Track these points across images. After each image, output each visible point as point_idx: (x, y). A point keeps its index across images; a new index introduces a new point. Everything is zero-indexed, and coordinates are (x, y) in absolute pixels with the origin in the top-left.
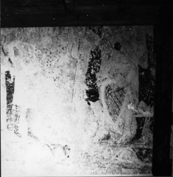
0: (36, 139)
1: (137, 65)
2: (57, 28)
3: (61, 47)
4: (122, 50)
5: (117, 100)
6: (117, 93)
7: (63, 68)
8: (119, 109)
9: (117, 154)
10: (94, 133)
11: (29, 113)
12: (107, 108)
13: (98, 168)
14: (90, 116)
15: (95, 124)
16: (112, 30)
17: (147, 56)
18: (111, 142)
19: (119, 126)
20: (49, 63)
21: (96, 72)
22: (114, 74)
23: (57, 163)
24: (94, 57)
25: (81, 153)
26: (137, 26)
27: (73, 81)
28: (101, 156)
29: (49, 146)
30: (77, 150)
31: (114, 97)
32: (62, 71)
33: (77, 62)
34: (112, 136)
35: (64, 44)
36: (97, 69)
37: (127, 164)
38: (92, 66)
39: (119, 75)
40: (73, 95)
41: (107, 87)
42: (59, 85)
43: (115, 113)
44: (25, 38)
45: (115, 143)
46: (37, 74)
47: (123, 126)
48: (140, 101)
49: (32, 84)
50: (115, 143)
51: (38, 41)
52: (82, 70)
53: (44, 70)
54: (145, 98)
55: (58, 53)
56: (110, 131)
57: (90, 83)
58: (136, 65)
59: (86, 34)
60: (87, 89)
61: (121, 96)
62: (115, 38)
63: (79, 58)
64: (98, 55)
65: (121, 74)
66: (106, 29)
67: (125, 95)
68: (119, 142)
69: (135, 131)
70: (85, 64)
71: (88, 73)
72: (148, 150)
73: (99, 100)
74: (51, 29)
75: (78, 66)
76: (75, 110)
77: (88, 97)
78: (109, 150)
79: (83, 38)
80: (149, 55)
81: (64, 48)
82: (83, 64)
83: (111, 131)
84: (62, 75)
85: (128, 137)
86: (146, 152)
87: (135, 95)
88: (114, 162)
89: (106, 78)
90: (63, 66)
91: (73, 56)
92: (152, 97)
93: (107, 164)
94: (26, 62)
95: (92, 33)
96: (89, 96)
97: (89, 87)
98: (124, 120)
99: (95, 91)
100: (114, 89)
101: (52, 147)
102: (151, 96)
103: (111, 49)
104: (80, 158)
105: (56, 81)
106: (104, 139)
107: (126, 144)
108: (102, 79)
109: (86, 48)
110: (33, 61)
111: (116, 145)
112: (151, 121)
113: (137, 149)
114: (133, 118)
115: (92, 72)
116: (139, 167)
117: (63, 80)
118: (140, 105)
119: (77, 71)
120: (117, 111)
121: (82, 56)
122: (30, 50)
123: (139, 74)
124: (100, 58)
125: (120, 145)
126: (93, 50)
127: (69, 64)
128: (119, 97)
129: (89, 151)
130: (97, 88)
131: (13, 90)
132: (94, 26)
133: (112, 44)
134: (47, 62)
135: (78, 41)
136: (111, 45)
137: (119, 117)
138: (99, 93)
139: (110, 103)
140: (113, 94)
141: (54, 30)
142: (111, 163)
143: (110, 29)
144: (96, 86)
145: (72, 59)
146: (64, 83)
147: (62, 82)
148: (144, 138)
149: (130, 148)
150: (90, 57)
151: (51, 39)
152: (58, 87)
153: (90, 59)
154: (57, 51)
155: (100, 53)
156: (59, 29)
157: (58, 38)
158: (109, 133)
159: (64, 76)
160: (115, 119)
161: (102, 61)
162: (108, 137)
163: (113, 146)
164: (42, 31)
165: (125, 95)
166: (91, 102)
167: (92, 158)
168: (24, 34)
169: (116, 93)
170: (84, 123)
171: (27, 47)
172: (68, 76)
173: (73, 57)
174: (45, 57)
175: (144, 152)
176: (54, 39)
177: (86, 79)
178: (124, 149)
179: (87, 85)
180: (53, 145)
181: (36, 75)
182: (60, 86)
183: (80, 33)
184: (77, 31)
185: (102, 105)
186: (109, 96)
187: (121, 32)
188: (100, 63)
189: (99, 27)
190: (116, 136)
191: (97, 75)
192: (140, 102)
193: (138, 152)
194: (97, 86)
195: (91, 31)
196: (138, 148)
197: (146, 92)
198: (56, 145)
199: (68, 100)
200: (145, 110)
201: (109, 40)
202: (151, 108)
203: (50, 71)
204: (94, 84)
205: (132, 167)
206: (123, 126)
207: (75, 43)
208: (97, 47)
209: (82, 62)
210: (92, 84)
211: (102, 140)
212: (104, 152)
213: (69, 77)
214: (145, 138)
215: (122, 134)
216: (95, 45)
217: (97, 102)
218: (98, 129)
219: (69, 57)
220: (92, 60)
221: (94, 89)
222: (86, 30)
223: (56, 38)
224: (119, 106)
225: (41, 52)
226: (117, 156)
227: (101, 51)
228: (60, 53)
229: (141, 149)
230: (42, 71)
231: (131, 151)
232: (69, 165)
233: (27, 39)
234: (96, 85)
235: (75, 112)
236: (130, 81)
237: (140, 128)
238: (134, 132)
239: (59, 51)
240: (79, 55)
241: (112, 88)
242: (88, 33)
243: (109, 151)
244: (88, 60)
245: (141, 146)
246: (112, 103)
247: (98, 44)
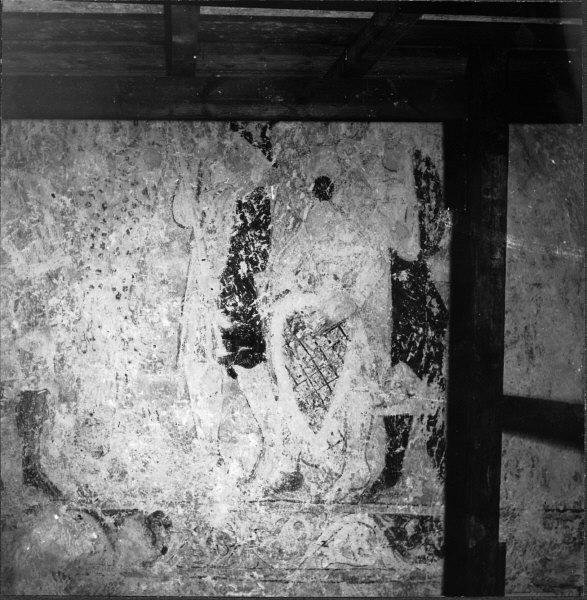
0: (53, 494)
2: (126, 124)
3: (140, 189)
4: (337, 198)
5: (323, 361)
6: (322, 340)
7: (144, 256)
8: (331, 391)
9: (325, 536)
10: (251, 468)
11: (28, 408)
12: (292, 386)
13: (261, 586)
14: (237, 413)
15: (253, 440)
16: (306, 134)
17: (416, 219)
18: (304, 497)
19: (331, 447)
20: (100, 239)
21: (256, 270)
22: (311, 275)
23: (126, 574)
24: (250, 222)
25: (208, 535)
26: (384, 126)
27: (179, 299)
28: (273, 546)
30: (194, 527)
31: (312, 353)
32: (141, 264)
33: (192, 237)
34: (309, 479)
35: (149, 178)
36: (257, 263)
37: (356, 568)
38: (242, 252)
39: (329, 281)
40: (179, 347)
41: (289, 321)
42: (133, 311)
43: (317, 404)
44: (14, 155)
45: (319, 500)
46: (56, 277)
48: (394, 362)
49: (41, 311)
50: (319, 500)
51: (62, 167)
52: (209, 265)
53: (82, 264)
54: (411, 354)
55: (129, 206)
56: (301, 463)
57: (235, 305)
58: (382, 248)
59: (221, 146)
60: (227, 324)
61: (334, 348)
62: (317, 159)
63: (199, 223)
64: (260, 214)
65: (336, 278)
66: (286, 131)
67: (349, 344)
68: (329, 497)
69: (382, 459)
70: (218, 245)
71: (227, 272)
72: (422, 519)
73: (265, 360)
74: (105, 126)
75: (198, 250)
76: (187, 396)
77: (230, 353)
78: (298, 525)
79: (210, 160)
80: (421, 216)
81: (150, 192)
82: (213, 243)
83: (304, 462)
84: (142, 279)
85: (360, 479)
86: (417, 528)
87: (381, 345)
88: (314, 565)
89: (288, 291)
90: (145, 251)
91: (177, 217)
92: (432, 349)
93: (293, 570)
94: (19, 234)
95: (242, 142)
96: (233, 349)
97: (232, 321)
98: (346, 426)
99: (253, 333)
100: (314, 325)
101: (109, 520)
102: (429, 348)
103: (302, 195)
104: (202, 554)
105: (122, 298)
106: (282, 488)
107: (353, 503)
108: (275, 293)
109: (220, 192)
110: (43, 234)
111: (322, 508)
112: (431, 428)
113: (389, 519)
114: (372, 417)
115: (240, 272)
116: (396, 577)
117: (148, 296)
118: (396, 377)
119: (192, 267)
120: (323, 398)
121: (210, 216)
122: (31, 194)
123: (392, 279)
124: (267, 224)
125: (333, 506)
126: (244, 201)
127: (168, 245)
128: (330, 352)
129: (234, 529)
130: (258, 323)
132: (247, 119)
133: (307, 181)
134: (92, 236)
135: (195, 168)
136: (301, 183)
137: (329, 415)
138: (266, 339)
139: (299, 371)
140: (309, 342)
141: (116, 130)
142: (305, 567)
143: (299, 131)
144: (254, 316)
145: (174, 228)
146: (150, 307)
147: (141, 303)
148: (408, 481)
149: (363, 515)
150: (236, 221)
151: (104, 162)
152: (130, 321)
153: (235, 227)
154: (126, 200)
155: (266, 208)
156: (131, 128)
157: (128, 159)
158: (298, 467)
159: (149, 282)
160: (315, 423)
161: (274, 234)
162: (295, 482)
163: (312, 512)
164: (74, 131)
165: (349, 344)
166: (238, 369)
167: (244, 552)
168: (11, 143)
169: (318, 337)
171: (22, 185)
172: (163, 282)
173: (180, 221)
174: (84, 220)
175: (410, 528)
176: (114, 159)
177: (224, 294)
178: (347, 519)
179: (227, 312)
180: (112, 513)
181: (55, 281)
182: (135, 316)
183: (203, 143)
184: (191, 135)
185: (275, 377)
186: (296, 347)
187: (336, 143)
188: (267, 240)
189: (264, 124)
190: (320, 476)
191: (259, 280)
192: (396, 367)
193: (392, 529)
194: (258, 317)
195: (237, 136)
196: (390, 516)
197: (415, 335)
198: (123, 514)
199: (162, 362)
200: (411, 392)
201: (297, 167)
202: (429, 385)
203: (103, 265)
204: (250, 309)
205: (374, 576)
206: (341, 445)
207: (185, 174)
208: (257, 189)
209: (209, 236)
210: (241, 309)
212: (283, 530)
213: (165, 287)
214: (414, 483)
215: (339, 472)
216: (251, 183)
217: (259, 367)
218: (261, 455)
219: (167, 221)
220: (243, 230)
221: (247, 327)
222: (221, 135)
223: (123, 157)
224: (330, 379)
225: (72, 202)
226: (325, 544)
227: (272, 204)
228: (135, 206)
229: (400, 519)
230: (75, 266)
231: (367, 526)
232: (166, 579)
233: (24, 159)
234: (257, 312)
235: (186, 401)
236: (363, 300)
237: (398, 451)
238: (378, 464)
239: (132, 200)
240: (199, 217)
241: (306, 321)
242: (228, 143)
243: (297, 529)
244: (230, 232)
245: (400, 510)
246: (307, 370)
247: (260, 178)
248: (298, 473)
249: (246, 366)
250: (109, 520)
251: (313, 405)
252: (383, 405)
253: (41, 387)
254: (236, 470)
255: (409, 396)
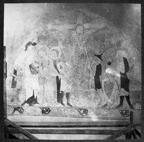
19: (112, 100)
29: (78, 109)
33: (90, 71)
72: (126, 111)
75: (91, 73)
76: (90, 93)
86: (125, 112)
101: (79, 110)
162: (106, 105)
166: (97, 89)
170: (94, 99)
175: (124, 112)
180: (79, 109)
211: (104, 106)
213: (86, 78)
229: (123, 111)
238: (119, 103)
245: (123, 109)
250: (79, 110)
251: (109, 95)
254: (97, 103)
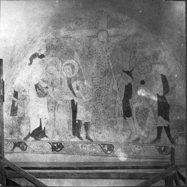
1: (156, 93)
4: (145, 84)
19: (146, 132)
32: (107, 98)
47: (148, 133)
72: (165, 147)
75: (118, 95)
76: (116, 123)
101: (102, 146)
131: (77, 111)
162: (138, 139)
166: (126, 118)
175: (163, 148)
180: (102, 144)
206: (148, 132)
213: (112, 103)
228: (105, 87)
229: (160, 147)
238: (156, 136)
248: (139, 138)
249: (128, 117)
250: (102, 146)
251: (142, 125)
252: (156, 124)
253: (89, 121)
255: (162, 122)
